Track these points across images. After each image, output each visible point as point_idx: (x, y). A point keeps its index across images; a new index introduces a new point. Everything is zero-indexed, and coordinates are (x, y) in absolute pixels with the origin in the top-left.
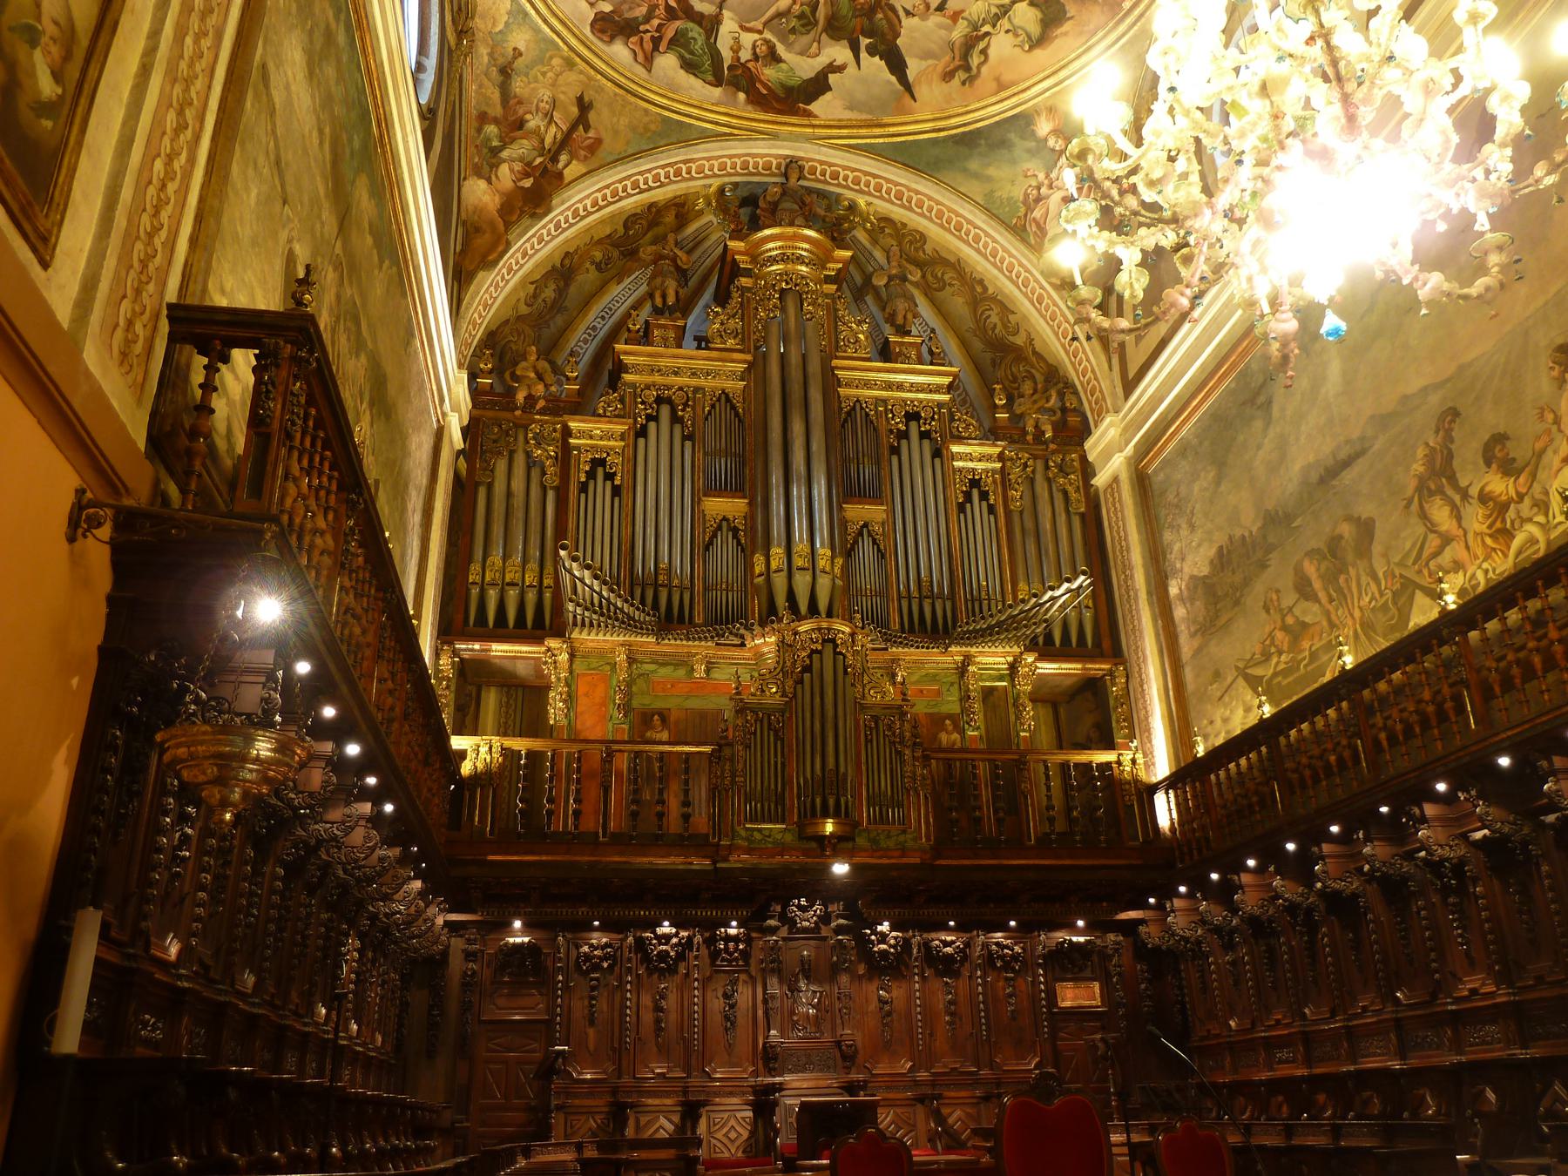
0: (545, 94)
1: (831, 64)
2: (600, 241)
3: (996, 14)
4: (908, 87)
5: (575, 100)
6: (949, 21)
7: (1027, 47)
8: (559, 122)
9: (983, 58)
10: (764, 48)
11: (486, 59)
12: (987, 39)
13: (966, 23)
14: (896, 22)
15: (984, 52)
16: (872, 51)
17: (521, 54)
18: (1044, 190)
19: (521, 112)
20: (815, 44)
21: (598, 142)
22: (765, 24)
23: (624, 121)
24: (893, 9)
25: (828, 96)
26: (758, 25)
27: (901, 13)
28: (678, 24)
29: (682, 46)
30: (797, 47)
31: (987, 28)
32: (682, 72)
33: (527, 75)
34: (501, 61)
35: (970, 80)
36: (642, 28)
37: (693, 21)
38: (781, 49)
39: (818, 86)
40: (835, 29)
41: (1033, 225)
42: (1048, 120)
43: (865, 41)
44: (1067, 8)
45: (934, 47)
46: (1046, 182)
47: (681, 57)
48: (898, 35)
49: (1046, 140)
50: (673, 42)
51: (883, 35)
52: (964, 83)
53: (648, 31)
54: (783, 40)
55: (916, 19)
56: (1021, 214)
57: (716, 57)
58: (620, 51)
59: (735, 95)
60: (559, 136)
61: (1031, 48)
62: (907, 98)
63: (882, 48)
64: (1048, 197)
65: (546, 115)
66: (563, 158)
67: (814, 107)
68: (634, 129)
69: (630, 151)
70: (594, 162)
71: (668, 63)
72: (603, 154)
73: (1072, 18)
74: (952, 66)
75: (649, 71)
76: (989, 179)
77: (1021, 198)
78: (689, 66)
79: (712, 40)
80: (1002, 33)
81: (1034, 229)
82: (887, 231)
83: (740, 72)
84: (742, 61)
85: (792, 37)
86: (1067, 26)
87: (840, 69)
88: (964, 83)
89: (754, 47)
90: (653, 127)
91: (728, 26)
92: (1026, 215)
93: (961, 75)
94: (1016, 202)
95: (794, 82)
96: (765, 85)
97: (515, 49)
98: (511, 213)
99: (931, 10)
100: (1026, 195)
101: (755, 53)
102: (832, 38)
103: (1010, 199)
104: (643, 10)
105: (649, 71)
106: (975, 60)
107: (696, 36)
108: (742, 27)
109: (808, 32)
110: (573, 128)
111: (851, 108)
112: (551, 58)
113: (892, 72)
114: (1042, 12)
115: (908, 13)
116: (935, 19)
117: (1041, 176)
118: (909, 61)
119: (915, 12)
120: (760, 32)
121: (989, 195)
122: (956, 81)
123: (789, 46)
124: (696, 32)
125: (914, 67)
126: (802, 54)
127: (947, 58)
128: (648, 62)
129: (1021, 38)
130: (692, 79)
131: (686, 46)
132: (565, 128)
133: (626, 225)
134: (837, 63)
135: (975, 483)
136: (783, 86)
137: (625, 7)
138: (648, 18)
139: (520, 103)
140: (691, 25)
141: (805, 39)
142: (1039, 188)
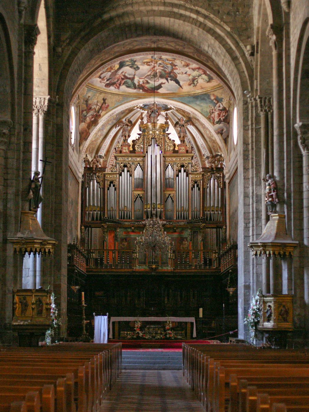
0: (95, 101)
2: (110, 120)
4: (181, 86)
10: (145, 81)
11: (82, 101)
16: (171, 80)
18: (214, 111)
19: (90, 106)
21: (108, 106)
22: (145, 77)
23: (114, 100)
24: (175, 73)
26: (144, 78)
27: (177, 74)
28: (125, 80)
29: (126, 84)
31: (197, 77)
33: (91, 99)
34: (86, 100)
35: (195, 86)
38: (149, 81)
39: (160, 86)
40: (161, 76)
45: (186, 80)
48: (177, 77)
49: (213, 100)
50: (123, 84)
51: (173, 77)
52: (194, 86)
54: (150, 79)
57: (134, 85)
58: (112, 88)
60: (99, 107)
62: (181, 88)
64: (215, 112)
66: (100, 111)
69: (116, 106)
70: (107, 111)
71: (123, 88)
72: (109, 108)
74: (190, 83)
75: (119, 89)
76: (201, 106)
77: (209, 112)
78: (128, 87)
81: (212, 119)
82: (181, 111)
85: (152, 79)
87: (164, 83)
88: (194, 86)
89: (143, 81)
90: (121, 99)
93: (192, 85)
96: (146, 88)
98: (90, 127)
100: (210, 111)
103: (206, 111)
104: (116, 80)
105: (119, 89)
106: (195, 82)
108: (140, 79)
110: (102, 104)
111: (168, 91)
115: (178, 74)
116: (185, 75)
117: (213, 108)
118: (180, 82)
121: (202, 110)
127: (189, 82)
128: (118, 88)
130: (129, 89)
132: (100, 105)
133: (116, 116)
135: (196, 182)
136: (151, 87)
138: (117, 81)
140: (127, 80)
142: (213, 110)
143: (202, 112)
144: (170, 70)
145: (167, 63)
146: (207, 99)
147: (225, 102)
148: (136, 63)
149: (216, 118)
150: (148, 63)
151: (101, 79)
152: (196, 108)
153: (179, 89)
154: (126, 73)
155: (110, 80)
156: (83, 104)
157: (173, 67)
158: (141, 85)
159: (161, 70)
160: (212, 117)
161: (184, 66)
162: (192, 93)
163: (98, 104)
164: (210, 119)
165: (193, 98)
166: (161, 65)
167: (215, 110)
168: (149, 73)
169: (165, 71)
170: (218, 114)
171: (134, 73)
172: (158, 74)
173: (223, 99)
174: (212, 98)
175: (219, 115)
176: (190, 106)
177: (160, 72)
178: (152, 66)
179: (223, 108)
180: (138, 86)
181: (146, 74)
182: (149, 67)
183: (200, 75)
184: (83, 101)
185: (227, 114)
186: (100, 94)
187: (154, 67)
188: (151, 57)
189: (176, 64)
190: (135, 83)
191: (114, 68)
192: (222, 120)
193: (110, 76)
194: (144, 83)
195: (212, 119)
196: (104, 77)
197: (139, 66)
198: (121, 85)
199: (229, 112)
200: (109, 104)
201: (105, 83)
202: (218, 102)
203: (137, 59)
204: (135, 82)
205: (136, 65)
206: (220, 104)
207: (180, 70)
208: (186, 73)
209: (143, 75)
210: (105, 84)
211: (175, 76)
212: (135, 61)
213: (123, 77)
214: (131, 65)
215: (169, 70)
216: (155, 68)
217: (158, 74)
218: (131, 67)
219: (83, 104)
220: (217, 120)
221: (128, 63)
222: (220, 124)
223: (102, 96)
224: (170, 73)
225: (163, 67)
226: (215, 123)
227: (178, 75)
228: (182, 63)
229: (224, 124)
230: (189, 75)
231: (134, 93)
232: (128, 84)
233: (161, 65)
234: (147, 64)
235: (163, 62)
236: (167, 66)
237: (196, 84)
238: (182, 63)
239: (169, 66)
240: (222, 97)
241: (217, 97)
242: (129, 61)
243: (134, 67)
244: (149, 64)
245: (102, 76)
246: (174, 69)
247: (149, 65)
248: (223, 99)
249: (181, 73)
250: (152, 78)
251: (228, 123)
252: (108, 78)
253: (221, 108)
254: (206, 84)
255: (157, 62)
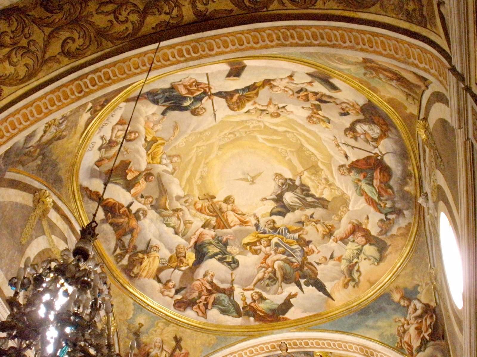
1: (290, 295)
3: (357, 253)
4: (329, 296)
5: (172, 339)
6: (338, 262)
7: (376, 263)
8: (167, 350)
9: (359, 274)
10: (257, 296)
11: (126, 331)
12: (357, 265)
13: (345, 261)
14: (314, 268)
15: (358, 271)
16: (307, 284)
17: (142, 325)
18: (406, 327)
19: (147, 349)
20: (280, 288)
22: (254, 286)
23: (198, 342)
25: (292, 309)
30: (272, 292)
31: (355, 260)
32: (221, 315)
33: (147, 333)
34: (133, 330)
35: (357, 285)
36: (198, 301)
37: (221, 292)
38: (264, 294)
39: (287, 305)
40: (287, 279)
41: (406, 345)
42: (397, 293)
43: (302, 281)
44: (386, 241)
45: (335, 275)
46: (406, 322)
47: (220, 309)
48: (316, 274)
49: (399, 303)
50: (214, 304)
51: (310, 276)
52: (354, 287)
53: (200, 302)
54: (265, 290)
55: (322, 266)
56: (399, 341)
59: (249, 320)
61: (378, 263)
62: (330, 299)
63: (312, 281)
64: (409, 329)
65: (160, 348)
67: (287, 315)
68: (203, 345)
71: (214, 313)
73: (390, 245)
74: (346, 281)
75: (206, 318)
76: (379, 328)
77: (397, 333)
78: (224, 312)
79: (232, 298)
80: (363, 260)
81: (406, 346)
83: (248, 309)
84: (248, 303)
85: (268, 288)
86: (390, 249)
87: (295, 296)
88: (354, 287)
89: (252, 296)
90: (213, 342)
91: (238, 291)
92: (401, 341)
93: (352, 284)
94: (394, 335)
95: (275, 307)
97: (139, 324)
99: (328, 259)
100: (399, 331)
101: (253, 299)
102: (287, 283)
105: (206, 318)
106: (356, 275)
107: (224, 298)
108: (245, 290)
109: (275, 283)
110: (174, 351)
111: (305, 311)
112: (158, 323)
113: (319, 291)
114: (376, 246)
115: (318, 264)
116: (331, 262)
117: (403, 320)
119: (321, 262)
120: (253, 290)
121: (381, 336)
122: (350, 287)
123: (268, 292)
124: (223, 296)
125: (329, 287)
126: (275, 293)
127: (343, 278)
128: (204, 315)
129: (372, 260)
130: (227, 317)
131: (220, 304)
132: (170, 352)
134: (293, 293)
136: (270, 310)
137: (188, 295)
138: (200, 297)
139: (146, 345)
140: (220, 295)
141: (274, 287)
142: (403, 326)
143: (383, 341)
144: (300, 259)
145: (291, 241)
146: (387, 306)
147: (424, 291)
148: (229, 249)
149: (415, 341)
150: (254, 247)
151: (161, 284)
152: (368, 336)
153: (326, 302)
154: (213, 276)
155: (183, 292)
156: (127, 337)
157: (305, 248)
158: (249, 305)
159: (282, 260)
160: (405, 342)
161: (324, 236)
162: (354, 304)
163: (165, 347)
164: (402, 348)
165: (359, 315)
166: (281, 249)
167: (408, 324)
168: (260, 275)
169: (291, 263)
170: (416, 329)
171: (229, 277)
172: (279, 274)
173: (418, 285)
174: (396, 297)
175: (419, 330)
176: (356, 335)
177: (281, 268)
178: (262, 255)
179: (423, 308)
180: (243, 308)
181: (254, 277)
182: (256, 257)
183: (360, 251)
184: (128, 333)
185: (434, 316)
186: (168, 325)
187: (268, 256)
188: (254, 228)
189: (307, 238)
190: (236, 303)
191: (185, 261)
192: (428, 338)
193: (181, 281)
194: (254, 301)
195: (405, 347)
196: (169, 281)
197: (237, 257)
198: (210, 306)
199: (437, 310)
200: (189, 351)
201: (172, 297)
202: (410, 300)
203: (228, 237)
204: (236, 300)
205: (230, 254)
206: (416, 302)
207: (319, 252)
208: (332, 257)
209: (249, 280)
210: (173, 302)
211: (313, 271)
212: (226, 244)
213: (210, 288)
214: (220, 256)
215: (297, 260)
216: (269, 261)
217: (279, 274)
218: (221, 260)
219: (127, 337)
220: (416, 344)
221: (213, 250)
222: (425, 349)
223: (170, 331)
224: (301, 267)
225: (283, 253)
226: (414, 353)
227: (318, 267)
228: (318, 231)
229: (433, 345)
230: (340, 259)
231: (240, 326)
232: (224, 306)
233: (281, 249)
234: (251, 248)
235: (282, 239)
236: (292, 250)
237: (357, 280)
238: (318, 231)
239: (295, 246)
240: (415, 282)
241: (405, 289)
242: (214, 242)
243: (227, 260)
244: (256, 248)
245: (164, 275)
246: (307, 254)
247: (256, 252)
248: (418, 285)
249: (323, 259)
250: (268, 285)
251: (443, 337)
252: (177, 287)
253: (419, 312)
254: (376, 267)
255: (270, 240)
